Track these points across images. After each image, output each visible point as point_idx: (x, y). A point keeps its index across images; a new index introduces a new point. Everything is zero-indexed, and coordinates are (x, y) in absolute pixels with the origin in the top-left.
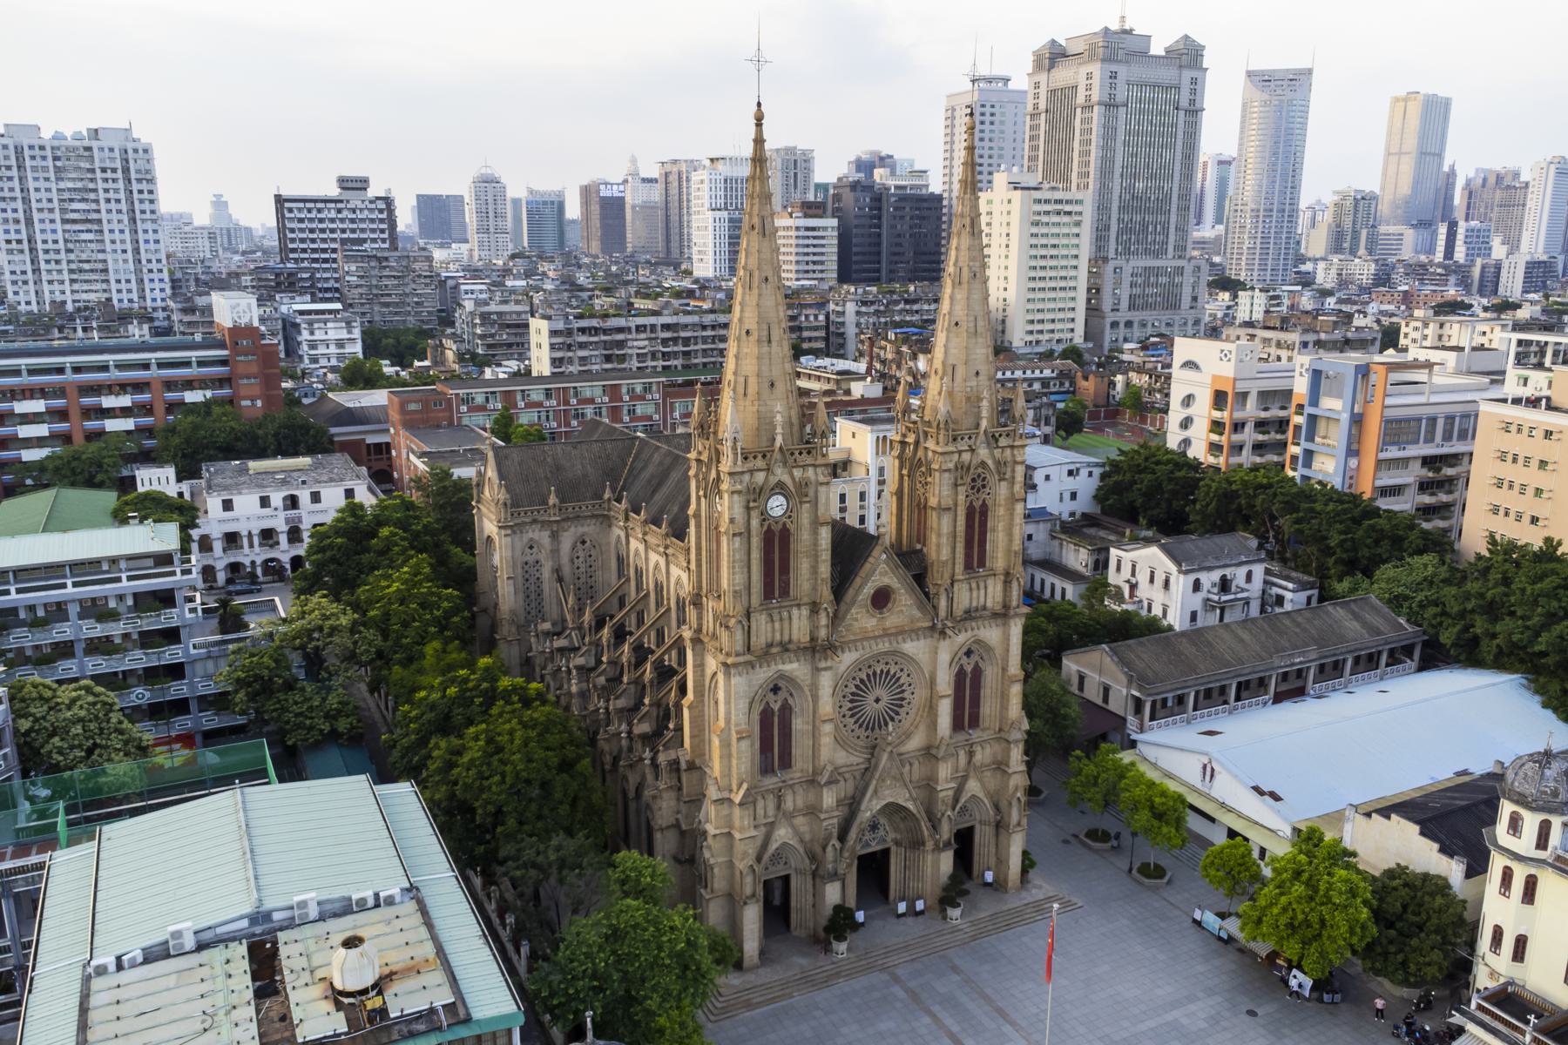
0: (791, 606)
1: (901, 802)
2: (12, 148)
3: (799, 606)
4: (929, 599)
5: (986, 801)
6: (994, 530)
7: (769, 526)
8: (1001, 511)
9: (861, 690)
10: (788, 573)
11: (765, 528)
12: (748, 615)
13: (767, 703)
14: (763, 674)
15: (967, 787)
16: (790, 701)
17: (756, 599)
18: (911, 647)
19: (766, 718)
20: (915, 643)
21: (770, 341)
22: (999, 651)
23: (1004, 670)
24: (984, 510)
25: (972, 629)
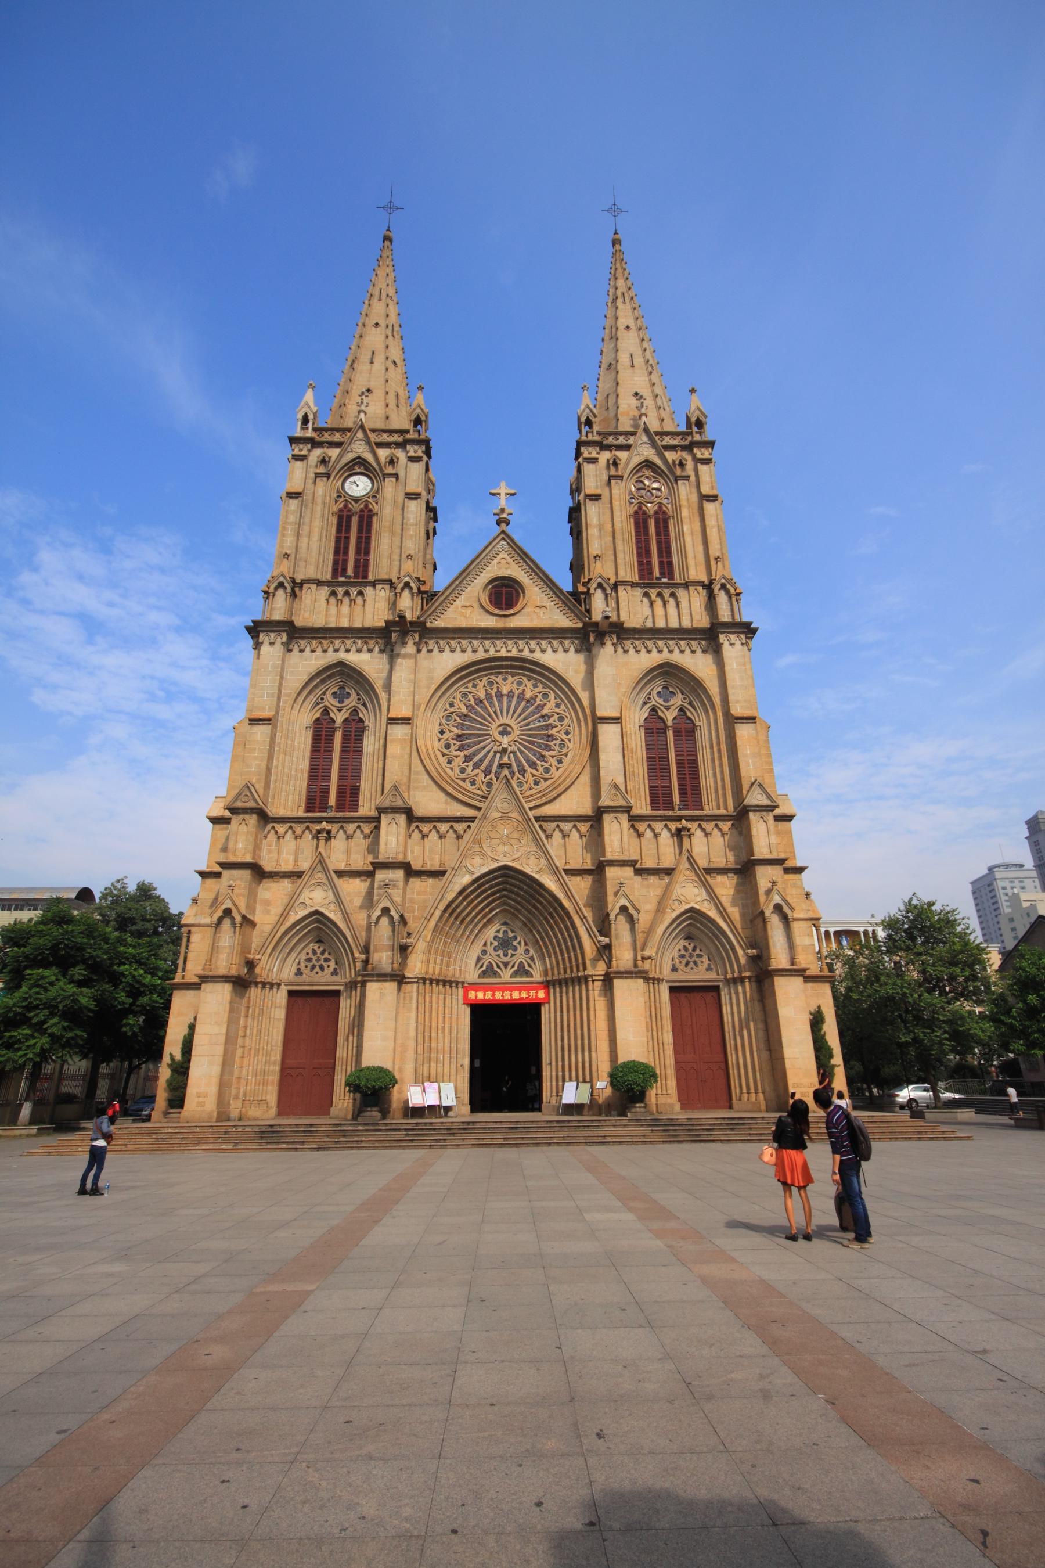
0: (366, 584)
1: (531, 867)
3: (374, 584)
6: (680, 535)
7: (346, 506)
8: (685, 512)
9: (476, 713)
10: (367, 553)
13: (326, 710)
15: (678, 891)
19: (322, 729)
20: (561, 655)
21: (372, 363)
22: (713, 687)
23: (727, 713)
24: (663, 519)
25: (660, 651)
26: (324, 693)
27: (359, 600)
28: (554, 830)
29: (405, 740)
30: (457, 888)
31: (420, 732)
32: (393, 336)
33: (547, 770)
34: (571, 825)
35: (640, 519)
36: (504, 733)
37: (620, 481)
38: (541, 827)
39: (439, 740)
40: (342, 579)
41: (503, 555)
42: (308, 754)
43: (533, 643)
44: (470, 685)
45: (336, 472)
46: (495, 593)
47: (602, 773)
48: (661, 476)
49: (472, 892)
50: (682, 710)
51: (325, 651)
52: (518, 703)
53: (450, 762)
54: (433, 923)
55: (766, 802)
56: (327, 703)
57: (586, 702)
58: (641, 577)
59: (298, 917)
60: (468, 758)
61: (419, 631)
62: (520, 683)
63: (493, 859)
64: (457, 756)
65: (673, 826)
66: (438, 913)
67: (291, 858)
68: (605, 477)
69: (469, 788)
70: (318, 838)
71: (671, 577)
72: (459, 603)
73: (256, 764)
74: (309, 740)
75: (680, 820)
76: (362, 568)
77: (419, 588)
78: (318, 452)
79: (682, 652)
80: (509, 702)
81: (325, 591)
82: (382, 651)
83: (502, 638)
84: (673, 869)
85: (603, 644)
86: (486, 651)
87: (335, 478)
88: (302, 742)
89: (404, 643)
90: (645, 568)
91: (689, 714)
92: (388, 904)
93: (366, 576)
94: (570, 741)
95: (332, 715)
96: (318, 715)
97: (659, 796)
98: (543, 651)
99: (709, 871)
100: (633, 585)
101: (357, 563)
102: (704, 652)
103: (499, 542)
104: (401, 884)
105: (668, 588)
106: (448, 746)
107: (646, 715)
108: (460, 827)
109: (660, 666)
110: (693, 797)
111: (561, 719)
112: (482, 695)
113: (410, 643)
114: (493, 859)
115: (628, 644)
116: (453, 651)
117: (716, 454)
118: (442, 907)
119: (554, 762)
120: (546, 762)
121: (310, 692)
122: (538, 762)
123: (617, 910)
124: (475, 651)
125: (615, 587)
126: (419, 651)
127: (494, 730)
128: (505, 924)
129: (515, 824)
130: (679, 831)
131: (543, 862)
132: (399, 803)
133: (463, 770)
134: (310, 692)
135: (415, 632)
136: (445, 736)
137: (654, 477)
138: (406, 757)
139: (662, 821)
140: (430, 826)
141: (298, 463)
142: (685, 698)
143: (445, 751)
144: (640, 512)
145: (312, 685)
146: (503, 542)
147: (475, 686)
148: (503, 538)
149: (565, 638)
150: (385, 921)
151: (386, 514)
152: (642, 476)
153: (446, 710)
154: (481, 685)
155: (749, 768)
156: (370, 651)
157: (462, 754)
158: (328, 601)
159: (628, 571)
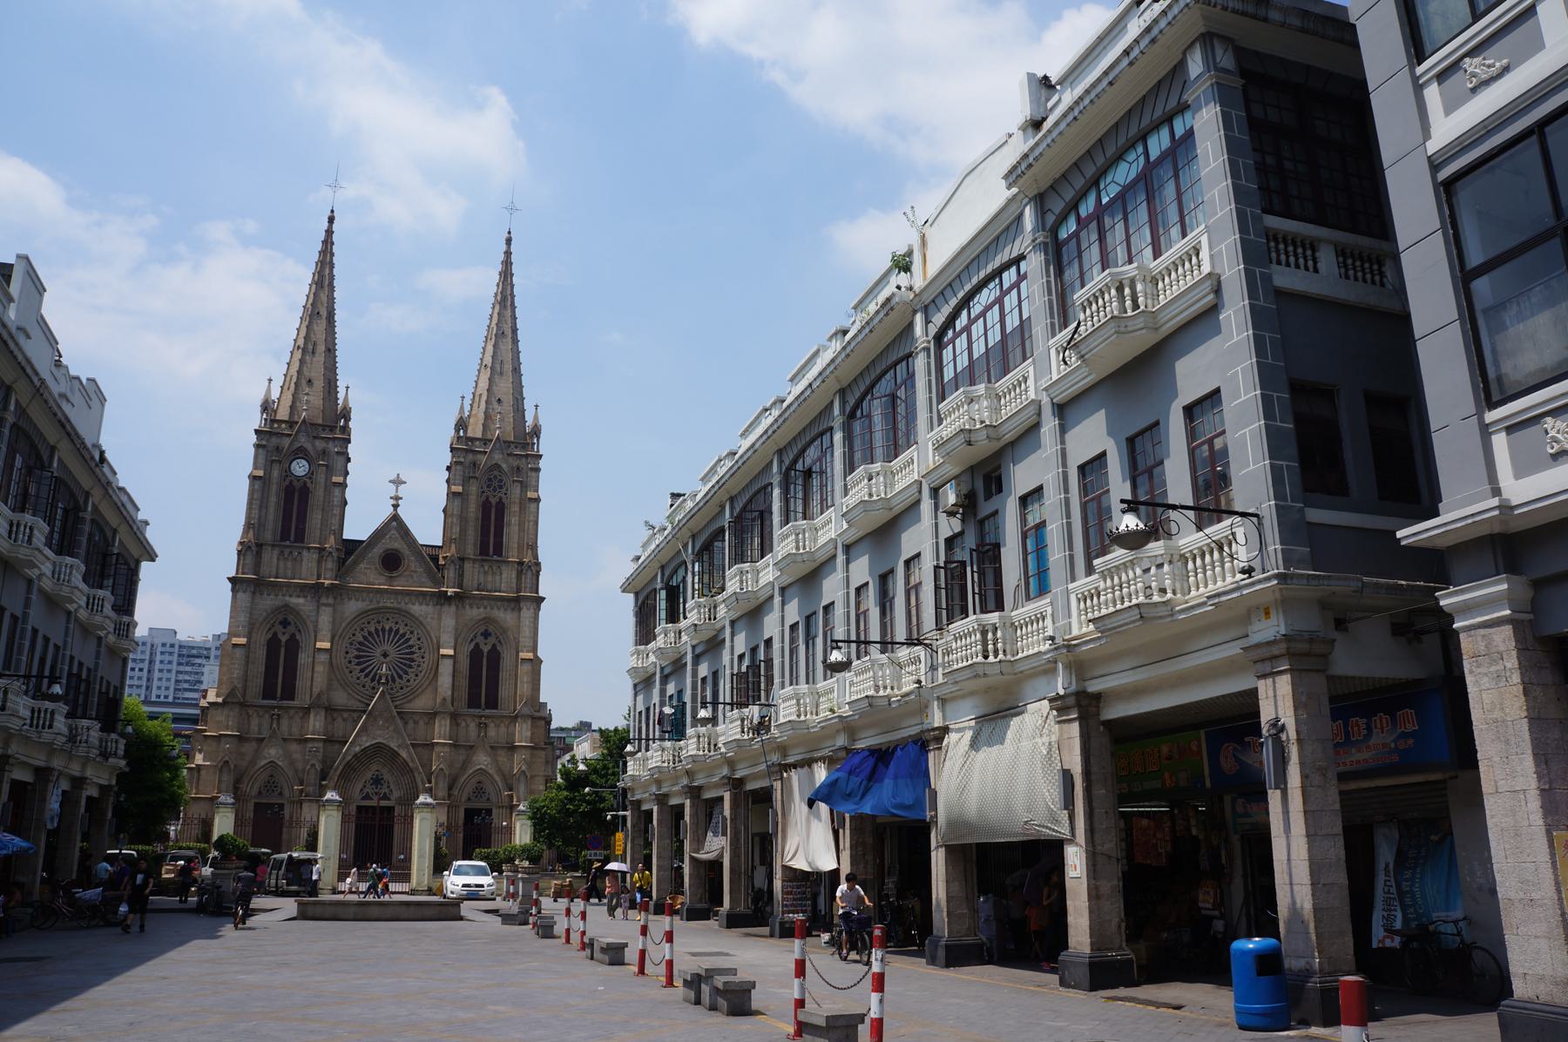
0: (303, 548)
1: (393, 745)
2: (149, 646)
4: (438, 569)
5: (497, 778)
6: (509, 524)
7: (291, 482)
10: (304, 523)
11: (287, 483)
12: (260, 546)
13: (275, 634)
14: (268, 602)
15: (474, 758)
16: (298, 637)
17: (268, 536)
18: (417, 609)
19: (273, 645)
20: (423, 607)
24: (501, 508)
25: (485, 608)
27: (299, 559)
30: (353, 754)
31: (334, 654)
33: (408, 681)
35: (486, 507)
36: (385, 655)
38: (401, 718)
40: (288, 543)
41: (392, 532)
47: (439, 690)
50: (494, 646)
51: (276, 595)
52: (395, 636)
54: (338, 773)
55: (529, 713)
57: (435, 641)
58: (481, 554)
59: (262, 764)
60: (362, 671)
62: (397, 623)
66: (341, 767)
67: (256, 729)
68: (467, 475)
69: (362, 689)
70: (272, 719)
71: (500, 555)
72: (362, 566)
73: (237, 672)
76: (300, 537)
77: (338, 558)
78: (274, 440)
79: (499, 609)
80: (389, 635)
81: (276, 552)
82: (312, 598)
85: (450, 605)
86: (378, 602)
88: (261, 654)
89: (328, 597)
90: (484, 550)
92: (313, 762)
93: (303, 541)
95: (280, 636)
96: (270, 636)
97: (473, 702)
98: (413, 604)
99: (491, 747)
100: (474, 561)
101: (297, 528)
102: (513, 610)
104: (321, 750)
106: (350, 662)
108: (356, 715)
109: (485, 618)
110: (493, 702)
111: (420, 649)
112: (373, 630)
113: (331, 596)
116: (357, 600)
117: (542, 464)
118: (344, 763)
119: (413, 676)
124: (371, 601)
125: (462, 559)
127: (378, 652)
131: (400, 741)
133: (358, 679)
136: (350, 655)
141: (261, 450)
146: (394, 523)
147: (369, 623)
150: (313, 771)
151: (318, 494)
154: (372, 623)
155: (524, 688)
156: (305, 597)
157: (359, 668)
158: (278, 559)
159: (471, 550)
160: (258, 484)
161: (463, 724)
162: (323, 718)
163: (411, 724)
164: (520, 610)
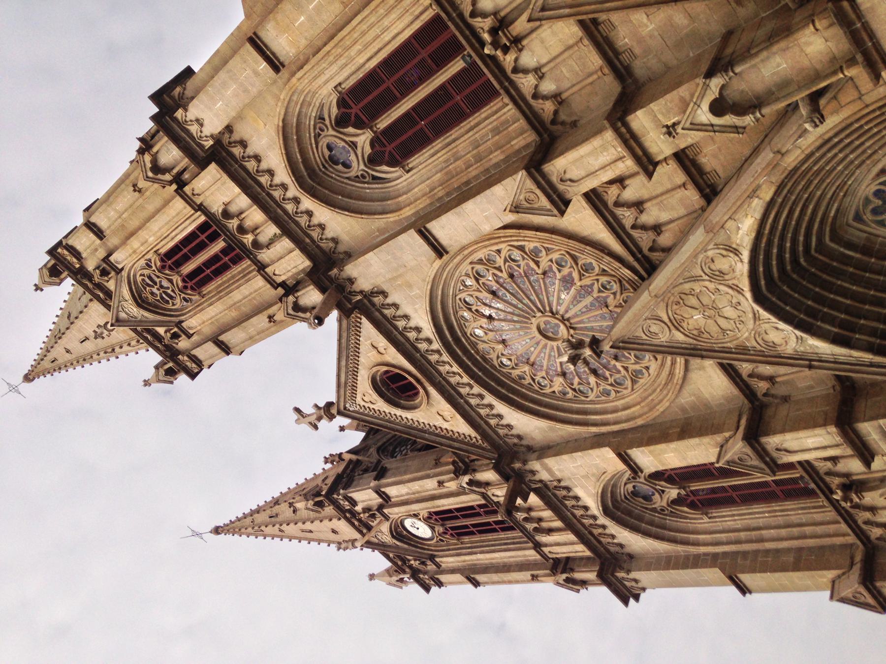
13: (675, 502)
20: (405, 309)
21: (311, 531)
25: (296, 200)
26: (654, 510)
28: (644, 228)
29: (650, 452)
32: (277, 515)
34: (620, 212)
37: (184, 325)
39: (618, 392)
41: (362, 403)
42: (744, 510)
43: (423, 346)
44: (526, 382)
45: (423, 551)
46: (402, 393)
48: (135, 282)
49: (832, 321)
53: (640, 372)
56: (664, 503)
61: (508, 465)
63: (756, 317)
64: (626, 369)
65: (508, 60)
72: (445, 425)
74: (725, 511)
75: (488, 55)
83: (444, 379)
84: (581, 23)
85: (351, 281)
87: (428, 550)
89: (533, 473)
91: (335, 111)
94: (499, 251)
98: (418, 330)
103: (349, 410)
105: (225, 227)
107: (385, 168)
113: (528, 467)
114: (756, 317)
115: (326, 245)
120: (550, 267)
121: (664, 527)
122: (559, 276)
123: (729, 119)
126: (530, 449)
128: (858, 218)
129: (675, 307)
130: (506, 50)
132: (748, 450)
134: (664, 527)
135: (513, 470)
137: (145, 289)
138: (673, 445)
139: (512, 82)
140: (753, 382)
142: (322, 130)
143: (628, 383)
144: (189, 285)
145: (654, 529)
146: (347, 405)
147: (521, 378)
148: (345, 408)
149: (384, 316)
152: (158, 301)
153: (575, 396)
160: (480, 578)
161: (548, 87)
162: (789, 436)
163: (652, 215)
164: (229, 129)
